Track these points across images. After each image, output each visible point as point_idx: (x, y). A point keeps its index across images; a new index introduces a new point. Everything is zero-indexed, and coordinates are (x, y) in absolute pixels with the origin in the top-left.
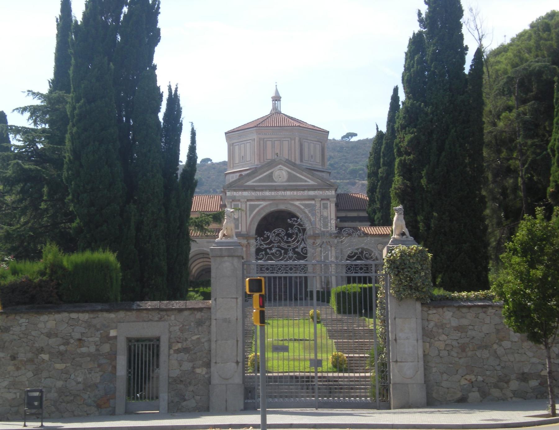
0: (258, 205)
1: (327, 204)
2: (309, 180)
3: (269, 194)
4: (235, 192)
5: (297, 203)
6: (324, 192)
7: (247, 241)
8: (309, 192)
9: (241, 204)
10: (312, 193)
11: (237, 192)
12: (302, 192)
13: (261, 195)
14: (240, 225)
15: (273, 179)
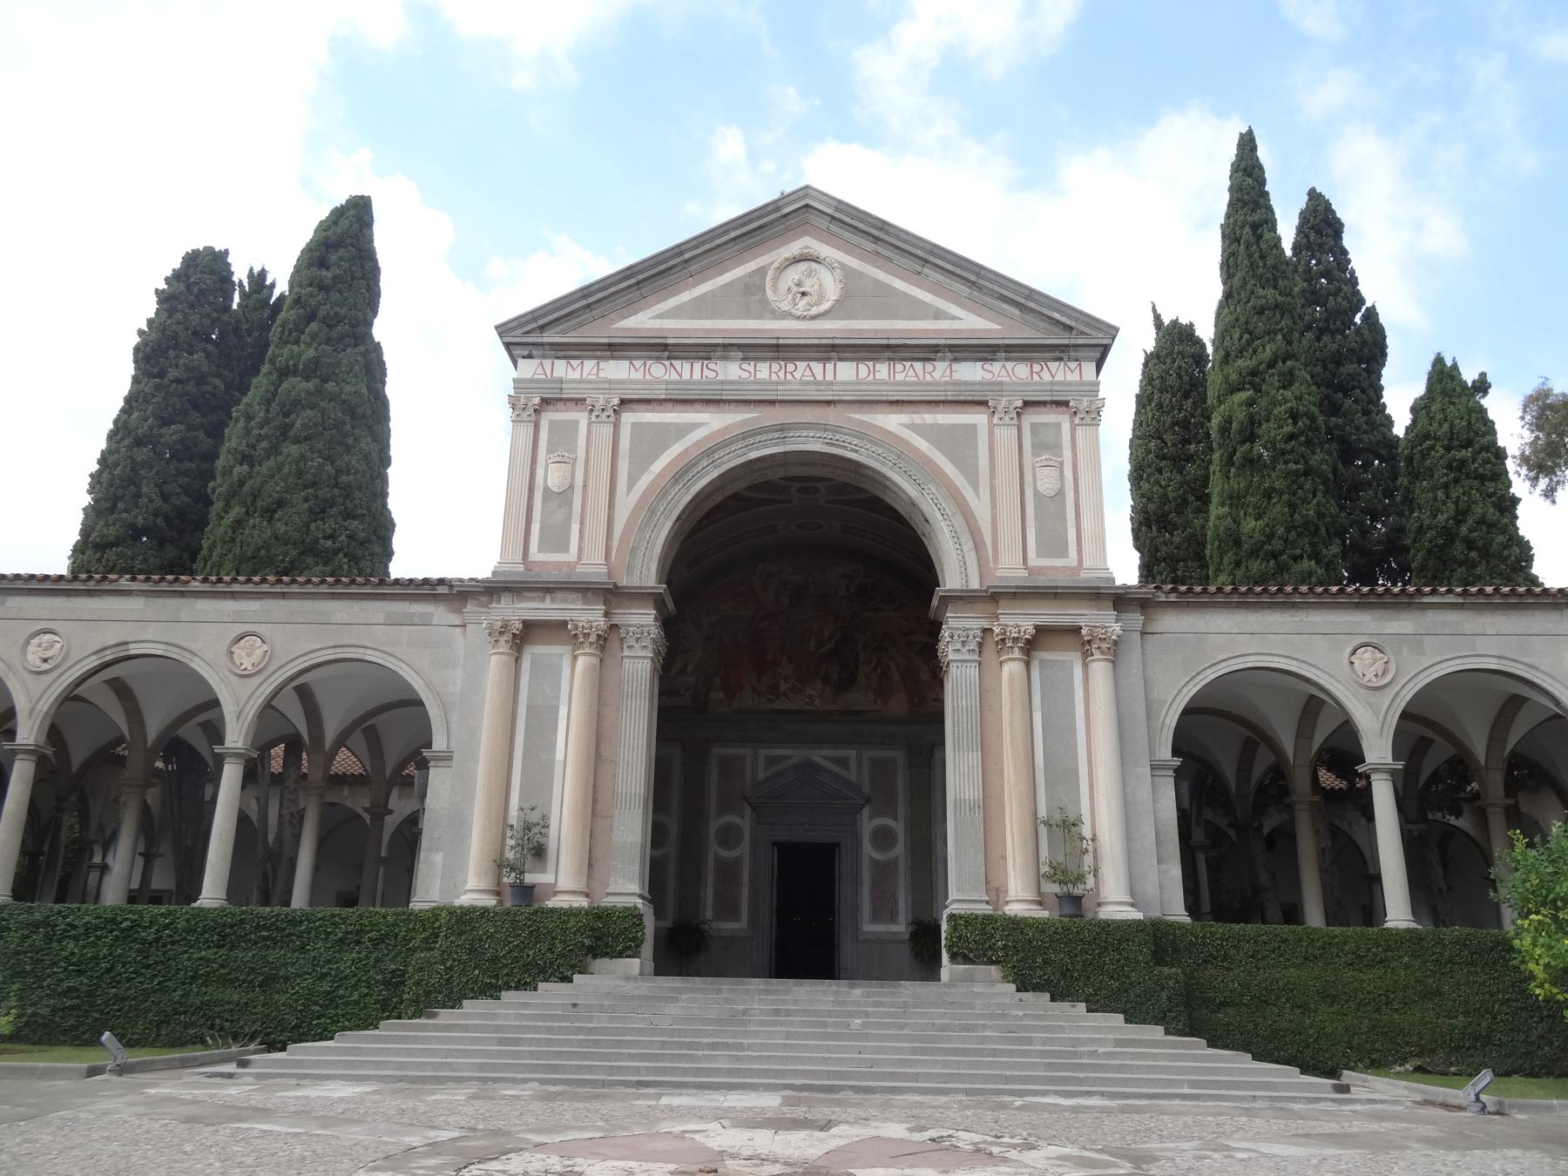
0: (682, 430)
1: (1058, 426)
2: (954, 309)
3: (745, 375)
4: (560, 365)
5: (892, 422)
6: (1036, 367)
7: (607, 614)
8: (956, 366)
9: (590, 424)
10: (971, 372)
11: (575, 363)
12: (918, 365)
13: (697, 376)
14: (575, 528)
15: (764, 302)
